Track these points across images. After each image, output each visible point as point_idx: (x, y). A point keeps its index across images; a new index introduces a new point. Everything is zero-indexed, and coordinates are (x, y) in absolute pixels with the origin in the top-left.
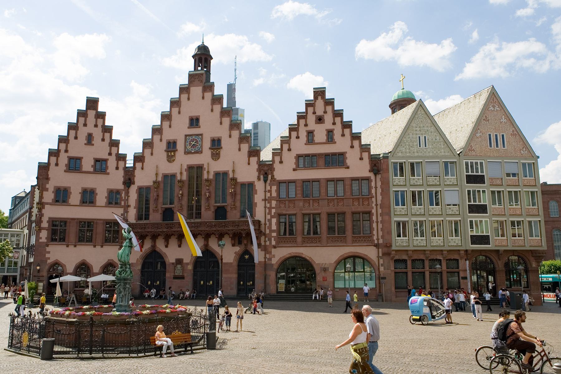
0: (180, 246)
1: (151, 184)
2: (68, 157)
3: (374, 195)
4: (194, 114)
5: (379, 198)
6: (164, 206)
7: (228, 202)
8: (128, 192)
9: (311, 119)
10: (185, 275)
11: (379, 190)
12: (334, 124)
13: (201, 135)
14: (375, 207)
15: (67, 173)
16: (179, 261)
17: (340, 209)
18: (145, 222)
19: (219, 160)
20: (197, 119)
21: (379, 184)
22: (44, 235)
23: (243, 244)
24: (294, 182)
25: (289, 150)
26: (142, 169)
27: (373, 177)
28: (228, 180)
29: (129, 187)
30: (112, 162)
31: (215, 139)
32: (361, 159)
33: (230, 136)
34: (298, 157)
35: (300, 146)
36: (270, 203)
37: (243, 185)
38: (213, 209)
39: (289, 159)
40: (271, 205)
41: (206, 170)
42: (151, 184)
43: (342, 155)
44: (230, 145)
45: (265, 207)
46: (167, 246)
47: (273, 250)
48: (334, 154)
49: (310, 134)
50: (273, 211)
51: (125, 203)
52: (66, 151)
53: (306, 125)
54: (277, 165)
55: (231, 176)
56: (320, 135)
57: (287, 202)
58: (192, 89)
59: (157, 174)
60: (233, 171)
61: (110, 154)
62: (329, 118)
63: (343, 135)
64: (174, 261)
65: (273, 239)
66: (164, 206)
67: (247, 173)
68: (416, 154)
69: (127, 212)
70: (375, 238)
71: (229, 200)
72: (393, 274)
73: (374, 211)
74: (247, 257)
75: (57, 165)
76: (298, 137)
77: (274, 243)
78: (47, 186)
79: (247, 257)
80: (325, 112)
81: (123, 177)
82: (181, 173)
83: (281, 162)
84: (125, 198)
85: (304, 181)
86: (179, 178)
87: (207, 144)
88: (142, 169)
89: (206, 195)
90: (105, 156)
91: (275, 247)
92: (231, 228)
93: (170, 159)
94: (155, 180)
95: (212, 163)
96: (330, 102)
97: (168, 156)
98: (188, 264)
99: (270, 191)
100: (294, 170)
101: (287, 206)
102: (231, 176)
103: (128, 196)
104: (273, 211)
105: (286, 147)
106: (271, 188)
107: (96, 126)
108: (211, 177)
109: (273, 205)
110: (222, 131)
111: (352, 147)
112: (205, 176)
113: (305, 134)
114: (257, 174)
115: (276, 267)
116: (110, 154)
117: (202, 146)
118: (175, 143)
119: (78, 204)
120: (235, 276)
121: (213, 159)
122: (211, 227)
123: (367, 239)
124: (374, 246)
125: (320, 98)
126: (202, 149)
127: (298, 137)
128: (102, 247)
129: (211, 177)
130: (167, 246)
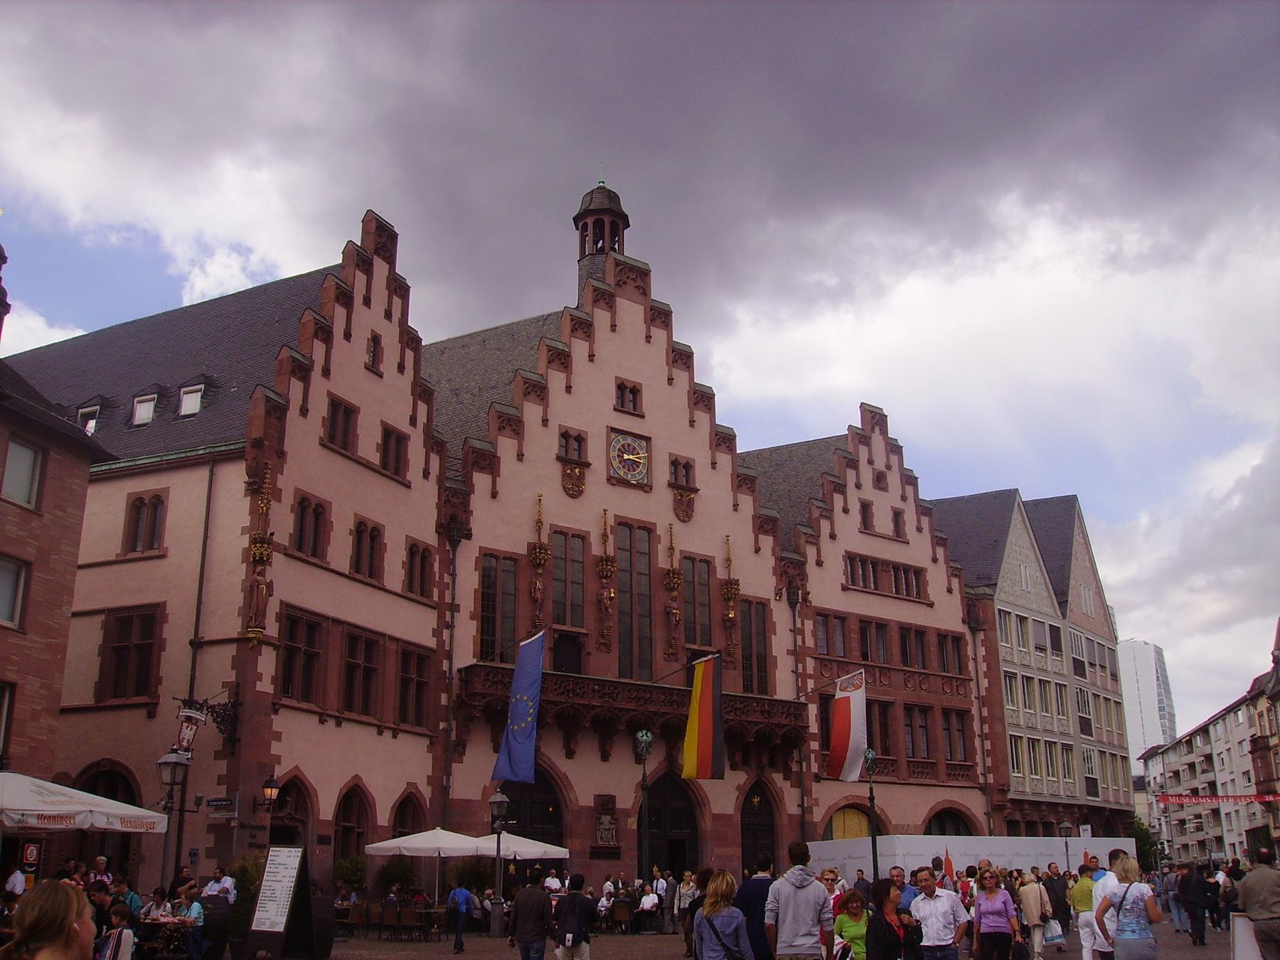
0: (605, 757)
1: (522, 550)
2: (330, 394)
3: (973, 675)
4: (631, 376)
5: (985, 683)
6: (556, 626)
8: (453, 562)
9: (867, 475)
10: (622, 844)
11: (983, 667)
12: (904, 498)
13: (648, 439)
14: (975, 702)
15: (325, 451)
16: (606, 804)
17: (925, 698)
18: (503, 665)
20: (635, 391)
21: (982, 651)
22: (267, 662)
24: (842, 617)
25: (833, 536)
26: (494, 495)
27: (968, 637)
29: (455, 544)
30: (416, 451)
32: (950, 591)
33: (714, 465)
34: (851, 558)
36: (804, 663)
37: (747, 601)
40: (804, 668)
42: (522, 550)
43: (919, 572)
44: (713, 485)
45: (795, 672)
46: (570, 754)
47: (815, 787)
48: (907, 569)
49: (866, 507)
50: (811, 684)
51: (442, 595)
52: (326, 372)
54: (811, 568)
55: (721, 574)
57: (834, 665)
58: (622, 304)
59: (539, 523)
60: (728, 561)
61: (413, 421)
63: (919, 530)
64: (591, 803)
65: (813, 756)
66: (556, 626)
67: (756, 576)
68: (1020, 602)
69: (450, 626)
70: (979, 770)
73: (974, 711)
74: (756, 800)
75: (304, 411)
76: (846, 511)
77: (815, 768)
78: (282, 482)
79: (756, 800)
80: (888, 467)
81: (438, 507)
82: (605, 536)
83: (819, 563)
84: (441, 577)
85: (865, 623)
86: (596, 550)
87: (662, 474)
88: (494, 495)
90: (403, 425)
91: (818, 778)
93: (574, 487)
94: (532, 538)
95: (678, 525)
96: (894, 448)
97: (565, 476)
98: (627, 813)
99: (801, 632)
100: (844, 588)
102: (721, 574)
103: (453, 575)
104: (811, 684)
105: (825, 526)
106: (803, 624)
107: (388, 315)
109: (810, 671)
110: (696, 448)
111: (935, 560)
112: (663, 562)
114: (772, 581)
116: (413, 421)
118: (580, 439)
119: (344, 565)
120: (739, 852)
123: (962, 772)
124: (980, 789)
125: (877, 429)
127: (846, 511)
128: (395, 737)
129: (676, 565)
130: (570, 754)
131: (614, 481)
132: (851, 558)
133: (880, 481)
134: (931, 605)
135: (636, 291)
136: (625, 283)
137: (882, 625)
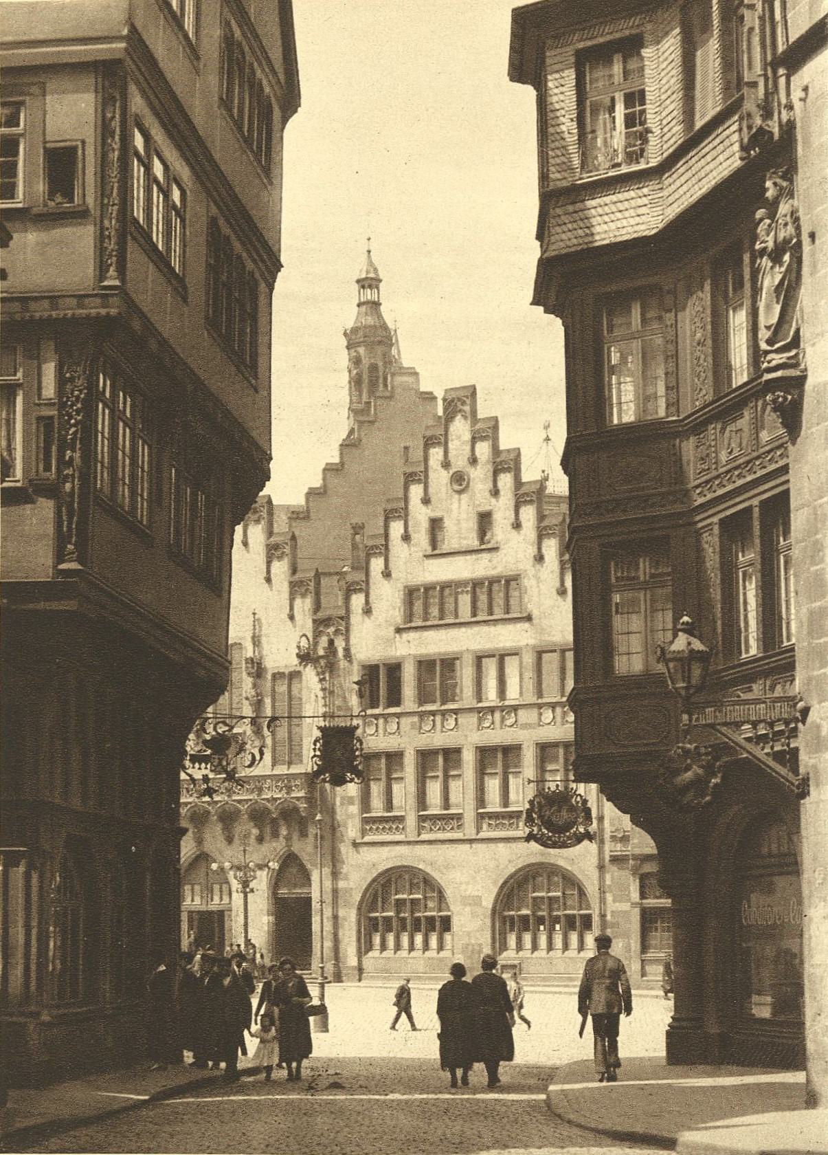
12: (495, 492)
23: (281, 838)
25: (387, 574)
34: (410, 593)
35: (410, 564)
39: (387, 597)
48: (493, 581)
49: (436, 525)
53: (426, 501)
54: (356, 618)
56: (461, 530)
60: (256, 641)
62: (479, 477)
63: (517, 525)
72: (636, 915)
76: (406, 538)
80: (473, 461)
83: (368, 611)
100: (399, 631)
101: (381, 731)
105: (377, 564)
111: (540, 558)
113: (425, 525)
115: (357, 897)
127: (406, 538)
132: (410, 593)
133: (459, 480)
134: (529, 618)
137: (449, 664)
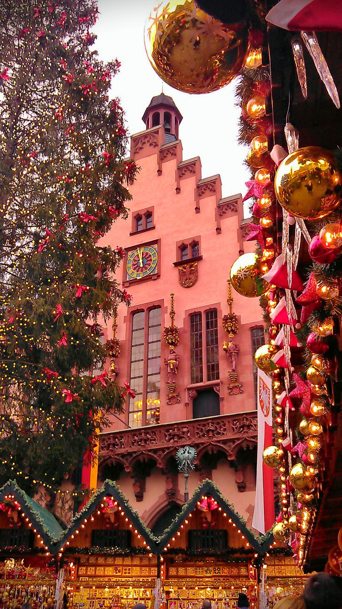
7: (221, 376)
19: (198, 284)
20: (149, 214)
28: (220, 322)
31: (186, 243)
38: (186, 397)
41: (169, 311)
71: (224, 372)
89: (167, 365)
92: (229, 435)
108: (180, 324)
117: (159, 265)
121: (182, 285)
122: (180, 438)
126: (159, 270)
129: (180, 324)
131: (128, 285)
135: (152, 147)
136: (141, 148)
